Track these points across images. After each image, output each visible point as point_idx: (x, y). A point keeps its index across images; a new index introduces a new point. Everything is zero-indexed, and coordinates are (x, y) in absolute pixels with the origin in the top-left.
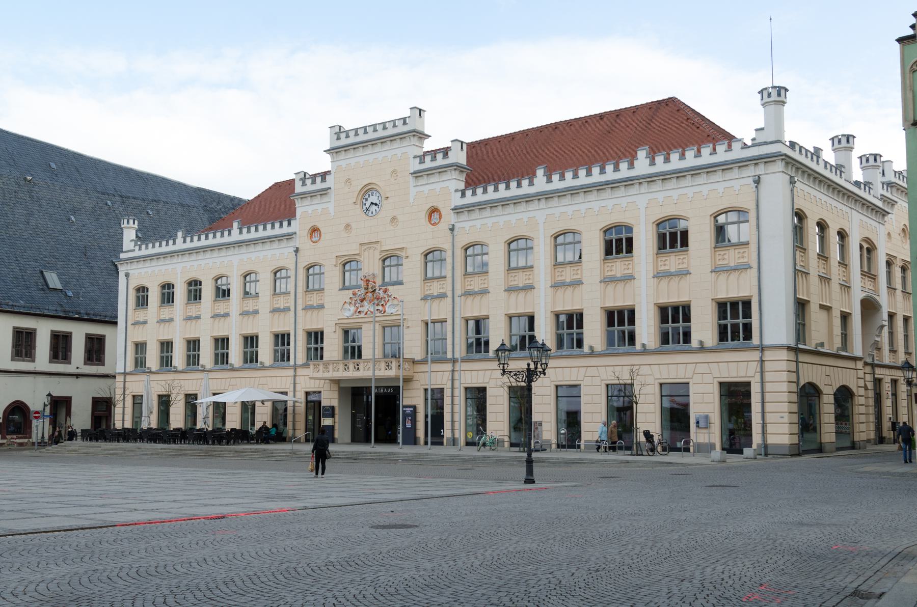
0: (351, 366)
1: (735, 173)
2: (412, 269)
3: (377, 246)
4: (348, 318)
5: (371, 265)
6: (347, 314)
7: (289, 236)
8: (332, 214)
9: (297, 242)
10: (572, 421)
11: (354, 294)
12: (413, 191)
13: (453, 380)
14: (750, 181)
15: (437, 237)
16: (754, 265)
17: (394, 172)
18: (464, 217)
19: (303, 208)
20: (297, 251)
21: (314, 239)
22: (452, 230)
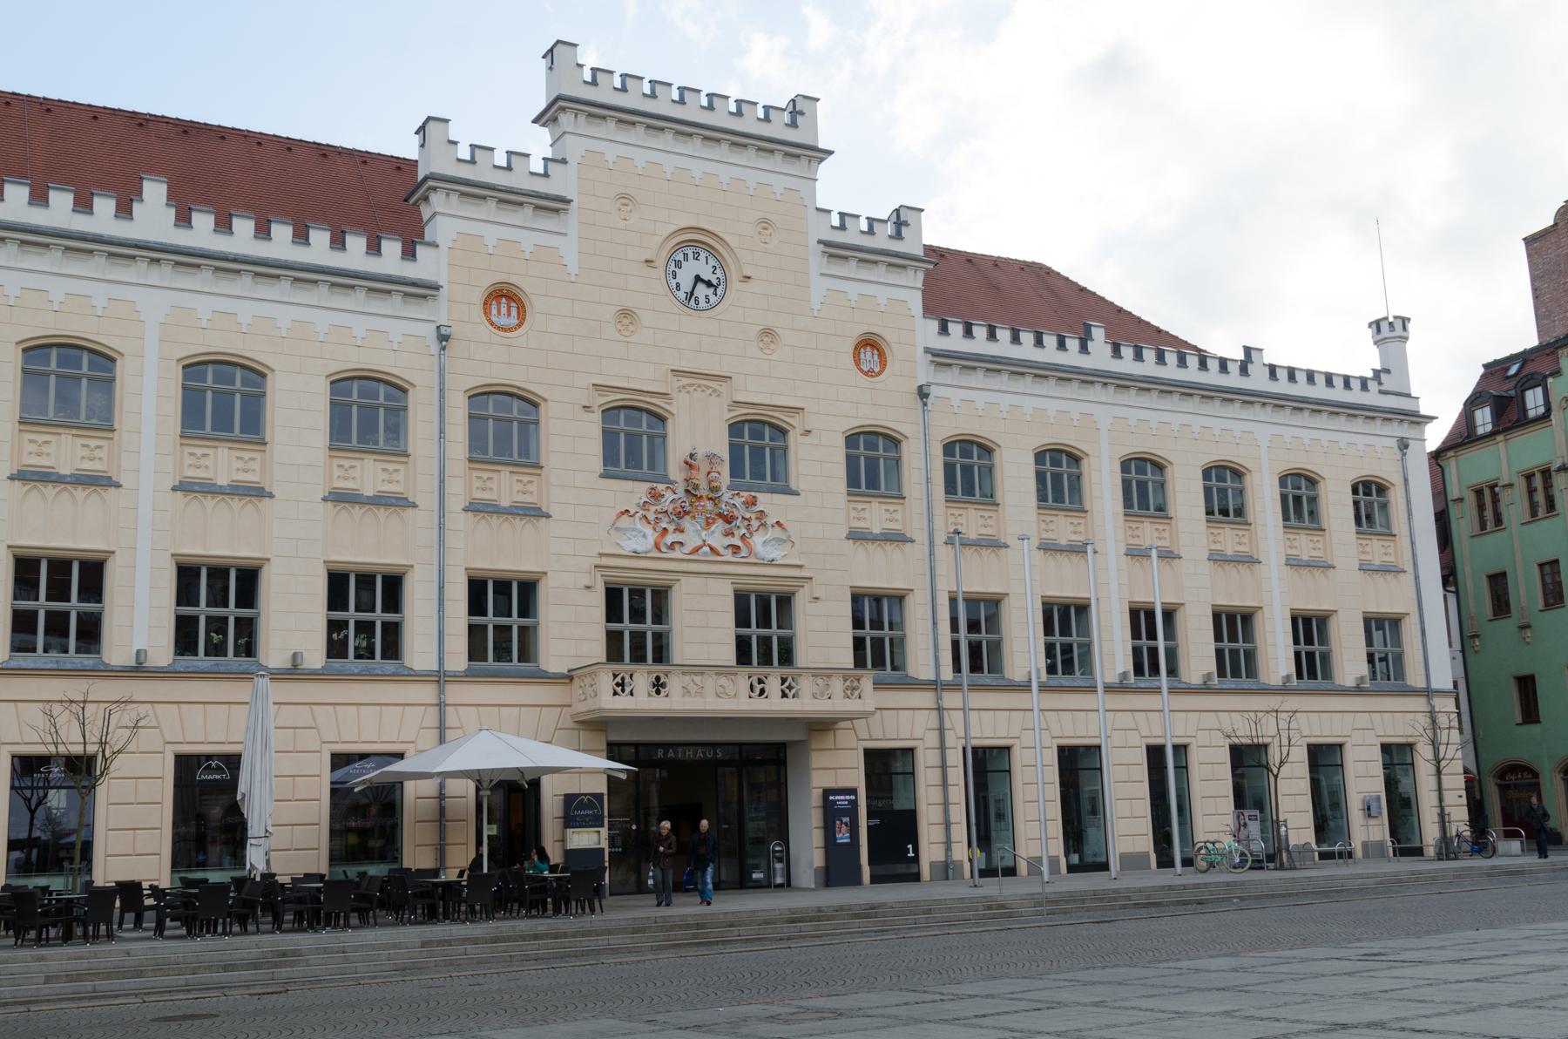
0: (773, 685)
1: (1377, 426)
2: (817, 461)
3: (723, 387)
4: (636, 555)
5: (698, 432)
6: (630, 545)
7: (423, 290)
8: (573, 268)
9: (440, 311)
10: (1400, 806)
11: (656, 496)
12: (819, 287)
13: (941, 730)
14: (1393, 443)
15: (881, 403)
16: (1409, 567)
17: (765, 223)
18: (951, 376)
19: (447, 220)
20: (443, 338)
21: (503, 321)
22: (923, 394)
